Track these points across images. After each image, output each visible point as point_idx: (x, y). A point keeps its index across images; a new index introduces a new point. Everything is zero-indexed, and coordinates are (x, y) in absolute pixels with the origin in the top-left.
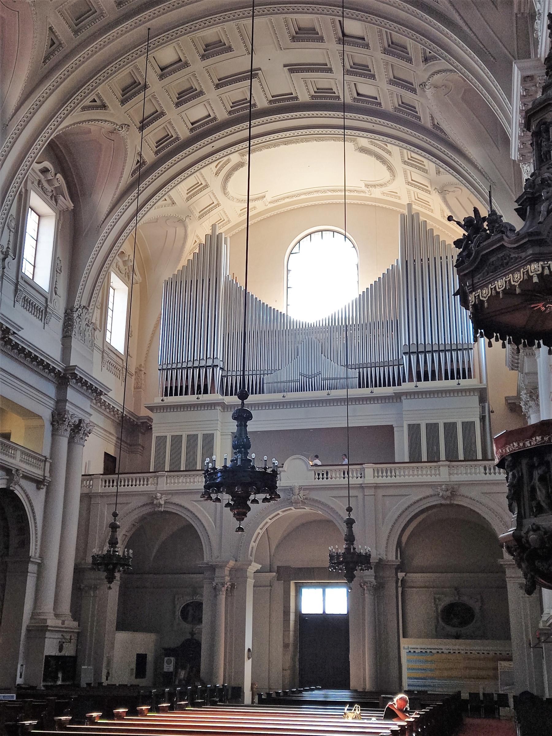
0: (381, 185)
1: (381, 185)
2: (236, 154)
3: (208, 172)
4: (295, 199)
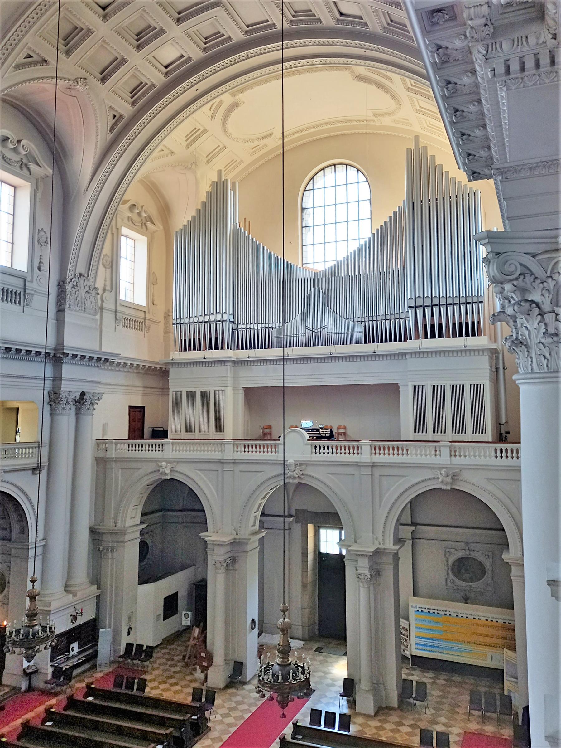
0: (389, 114)
1: (389, 114)
2: (227, 94)
3: (201, 116)
4: (304, 133)
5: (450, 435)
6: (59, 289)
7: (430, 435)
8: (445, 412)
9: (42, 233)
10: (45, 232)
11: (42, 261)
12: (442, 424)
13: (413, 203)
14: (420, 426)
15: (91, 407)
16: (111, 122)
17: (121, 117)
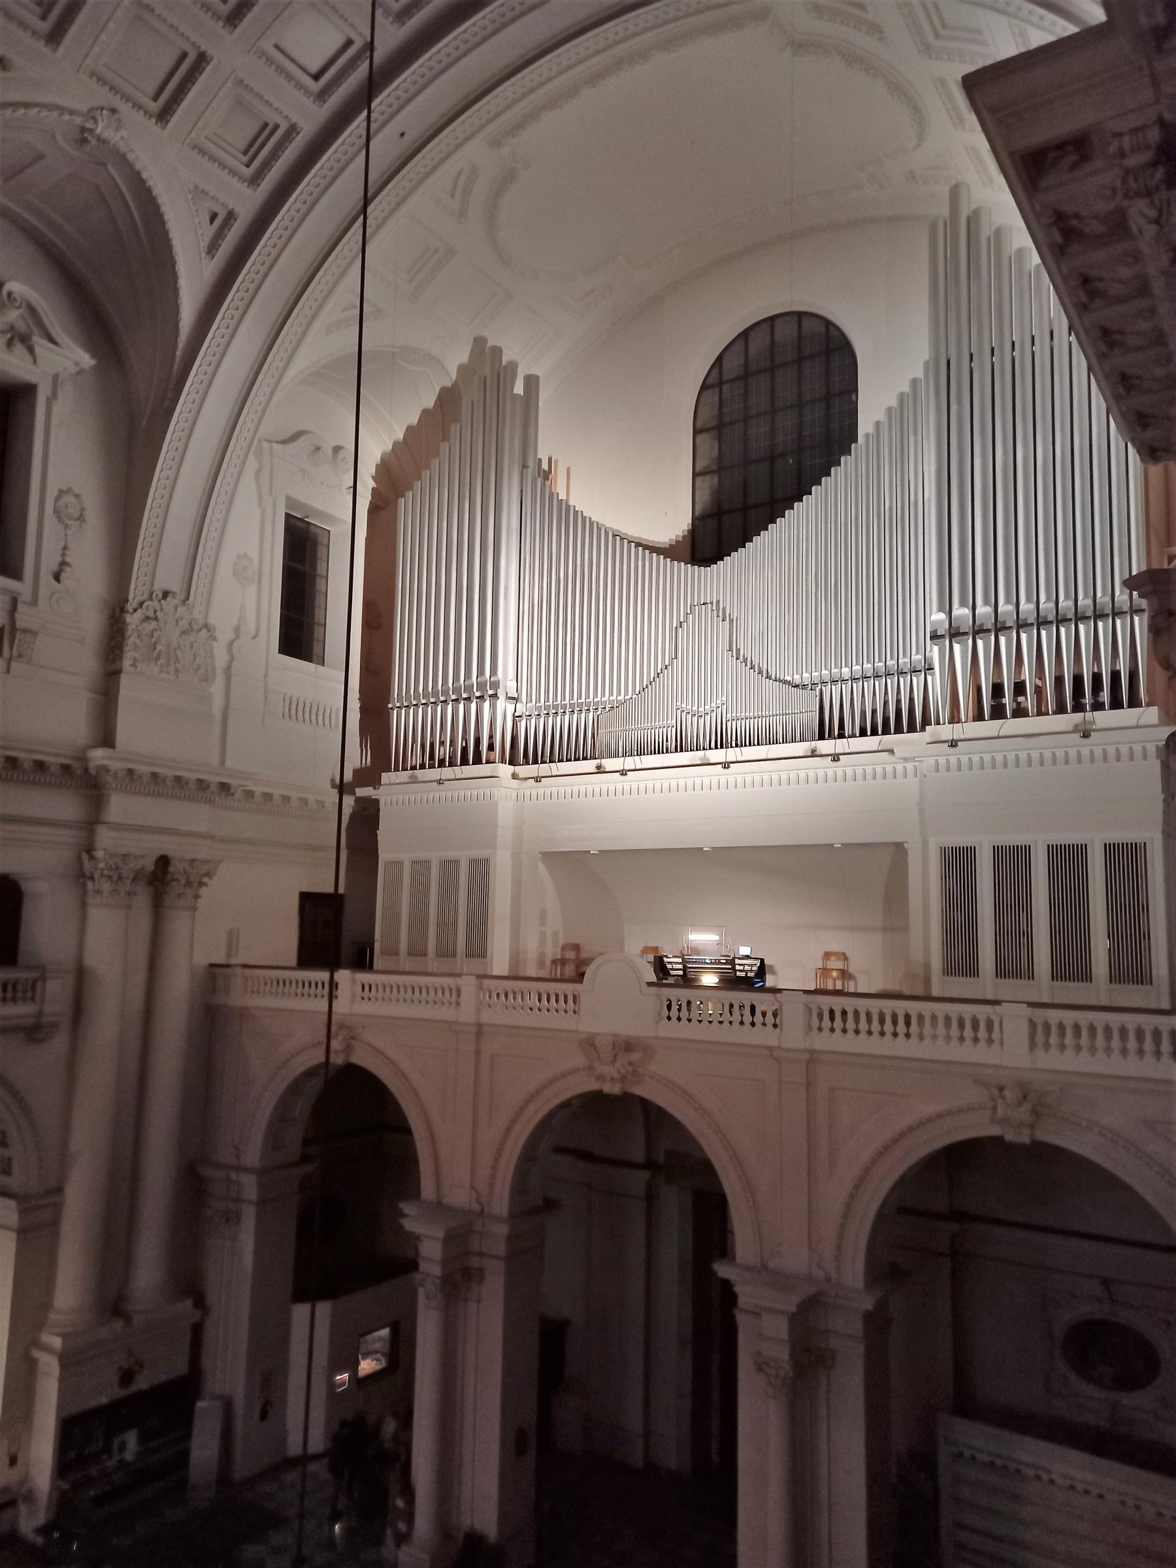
5: (1043, 985)
6: (112, 625)
7: (987, 982)
8: (1030, 923)
9: (69, 499)
10: (77, 496)
11: (68, 559)
12: (1024, 952)
13: (948, 362)
14: (961, 961)
15: (189, 892)
16: (211, 230)
17: (231, 216)
